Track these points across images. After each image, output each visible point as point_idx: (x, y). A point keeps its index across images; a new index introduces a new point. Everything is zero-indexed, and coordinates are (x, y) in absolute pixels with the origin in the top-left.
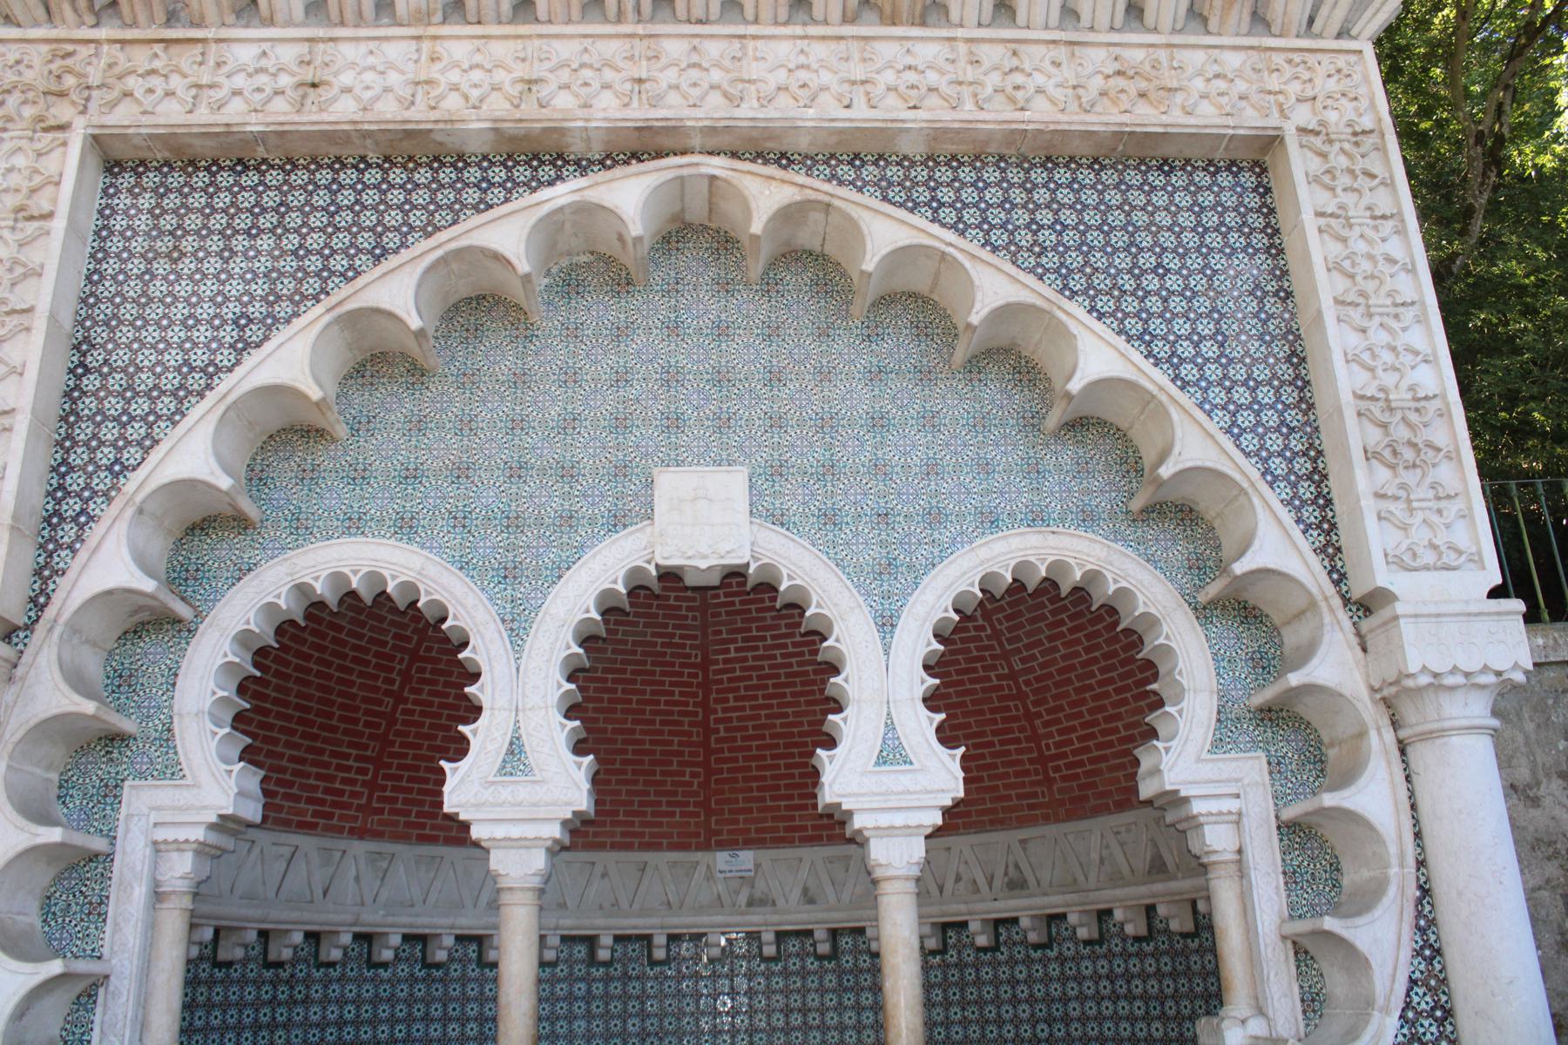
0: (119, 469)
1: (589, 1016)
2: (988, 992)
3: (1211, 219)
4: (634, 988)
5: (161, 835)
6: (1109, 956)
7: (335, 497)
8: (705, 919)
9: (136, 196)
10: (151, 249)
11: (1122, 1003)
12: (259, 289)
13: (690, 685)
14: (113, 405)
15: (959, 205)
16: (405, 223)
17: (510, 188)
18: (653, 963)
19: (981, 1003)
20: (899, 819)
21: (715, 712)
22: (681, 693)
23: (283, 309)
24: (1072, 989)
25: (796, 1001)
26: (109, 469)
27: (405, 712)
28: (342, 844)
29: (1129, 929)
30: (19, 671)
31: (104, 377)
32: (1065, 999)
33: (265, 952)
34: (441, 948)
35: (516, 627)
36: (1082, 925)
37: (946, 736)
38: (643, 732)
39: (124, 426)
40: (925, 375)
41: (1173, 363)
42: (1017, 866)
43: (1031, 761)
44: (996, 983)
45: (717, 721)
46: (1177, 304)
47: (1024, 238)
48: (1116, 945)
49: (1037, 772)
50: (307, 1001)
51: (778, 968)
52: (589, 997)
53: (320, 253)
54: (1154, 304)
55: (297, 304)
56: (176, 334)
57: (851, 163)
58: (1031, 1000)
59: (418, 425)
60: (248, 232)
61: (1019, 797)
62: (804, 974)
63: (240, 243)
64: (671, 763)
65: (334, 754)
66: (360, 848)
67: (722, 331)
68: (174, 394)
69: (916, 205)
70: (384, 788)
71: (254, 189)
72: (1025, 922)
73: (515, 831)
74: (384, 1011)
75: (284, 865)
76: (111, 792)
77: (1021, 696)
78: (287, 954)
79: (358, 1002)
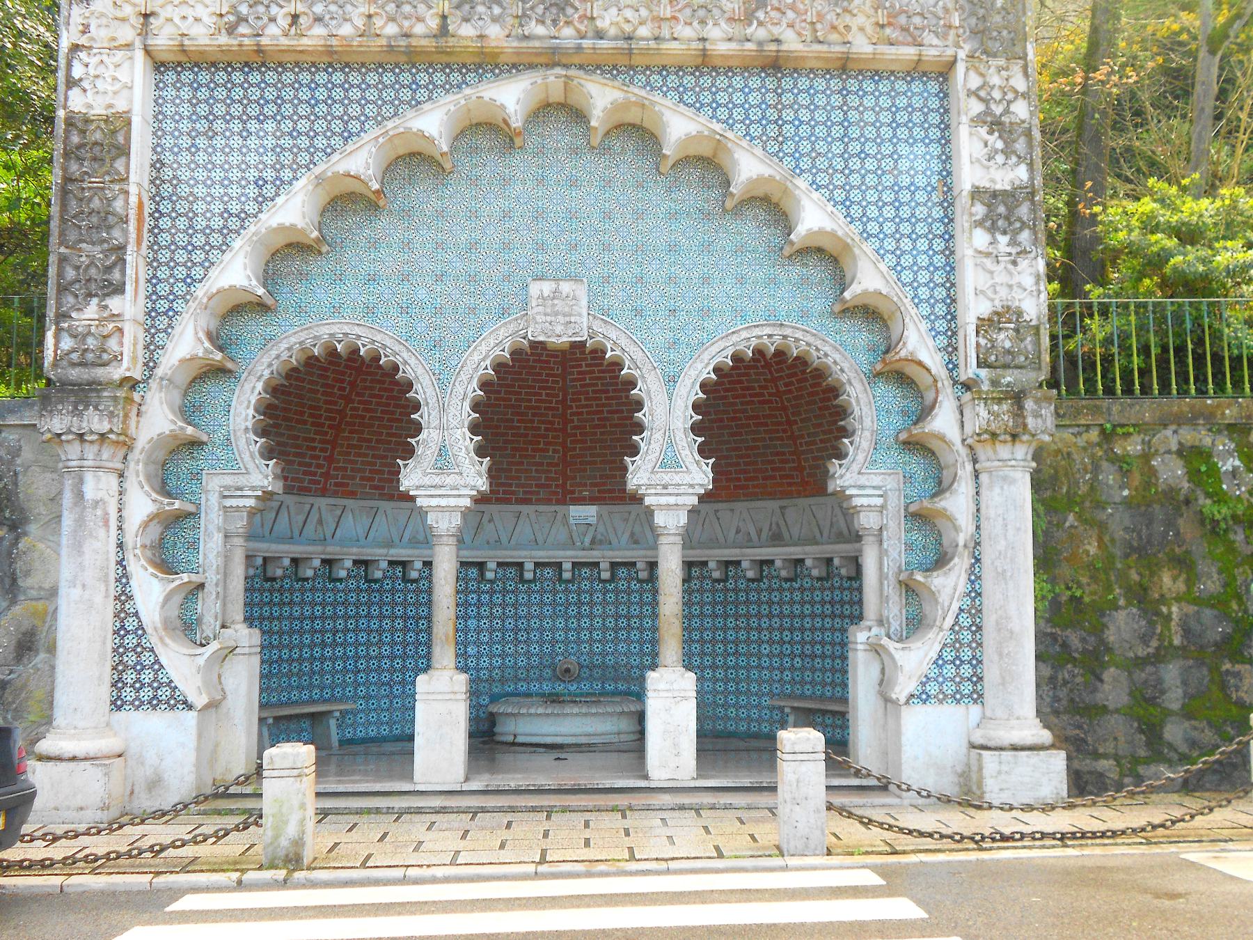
0: (190, 281)
1: (479, 617)
2: (753, 609)
3: (902, 117)
4: (510, 598)
5: (228, 503)
6: (832, 589)
7: (321, 294)
8: (561, 553)
9: (178, 90)
10: (193, 129)
11: (838, 620)
12: (269, 159)
13: (553, 389)
14: (182, 239)
15: (731, 106)
16: (363, 114)
17: (432, 87)
18: (522, 580)
19: (748, 616)
20: (672, 500)
21: (571, 407)
22: (547, 395)
23: (287, 174)
25: (623, 610)
27: (353, 409)
28: (311, 500)
29: (843, 572)
30: (143, 408)
31: (174, 219)
32: (802, 616)
33: (265, 571)
34: (378, 569)
35: (442, 385)
36: (815, 567)
37: (703, 451)
38: (519, 421)
39: (190, 253)
40: (707, 216)
41: (864, 219)
42: (778, 524)
43: (791, 453)
44: (759, 603)
45: (572, 414)
46: (871, 180)
47: (772, 130)
48: (836, 582)
49: (793, 461)
50: (291, 603)
51: (611, 587)
52: (479, 604)
54: (855, 179)
55: (295, 171)
56: (217, 191)
57: (660, 73)
58: (781, 616)
59: (374, 244)
60: (257, 118)
61: (782, 477)
62: (629, 592)
64: (539, 443)
65: (305, 439)
66: (322, 502)
67: (573, 183)
68: (220, 231)
69: (702, 105)
70: (339, 461)
71: (258, 85)
72: (778, 563)
73: (443, 502)
74: (341, 610)
75: (273, 515)
76: (196, 476)
77: (784, 409)
78: (279, 572)
79: (323, 605)
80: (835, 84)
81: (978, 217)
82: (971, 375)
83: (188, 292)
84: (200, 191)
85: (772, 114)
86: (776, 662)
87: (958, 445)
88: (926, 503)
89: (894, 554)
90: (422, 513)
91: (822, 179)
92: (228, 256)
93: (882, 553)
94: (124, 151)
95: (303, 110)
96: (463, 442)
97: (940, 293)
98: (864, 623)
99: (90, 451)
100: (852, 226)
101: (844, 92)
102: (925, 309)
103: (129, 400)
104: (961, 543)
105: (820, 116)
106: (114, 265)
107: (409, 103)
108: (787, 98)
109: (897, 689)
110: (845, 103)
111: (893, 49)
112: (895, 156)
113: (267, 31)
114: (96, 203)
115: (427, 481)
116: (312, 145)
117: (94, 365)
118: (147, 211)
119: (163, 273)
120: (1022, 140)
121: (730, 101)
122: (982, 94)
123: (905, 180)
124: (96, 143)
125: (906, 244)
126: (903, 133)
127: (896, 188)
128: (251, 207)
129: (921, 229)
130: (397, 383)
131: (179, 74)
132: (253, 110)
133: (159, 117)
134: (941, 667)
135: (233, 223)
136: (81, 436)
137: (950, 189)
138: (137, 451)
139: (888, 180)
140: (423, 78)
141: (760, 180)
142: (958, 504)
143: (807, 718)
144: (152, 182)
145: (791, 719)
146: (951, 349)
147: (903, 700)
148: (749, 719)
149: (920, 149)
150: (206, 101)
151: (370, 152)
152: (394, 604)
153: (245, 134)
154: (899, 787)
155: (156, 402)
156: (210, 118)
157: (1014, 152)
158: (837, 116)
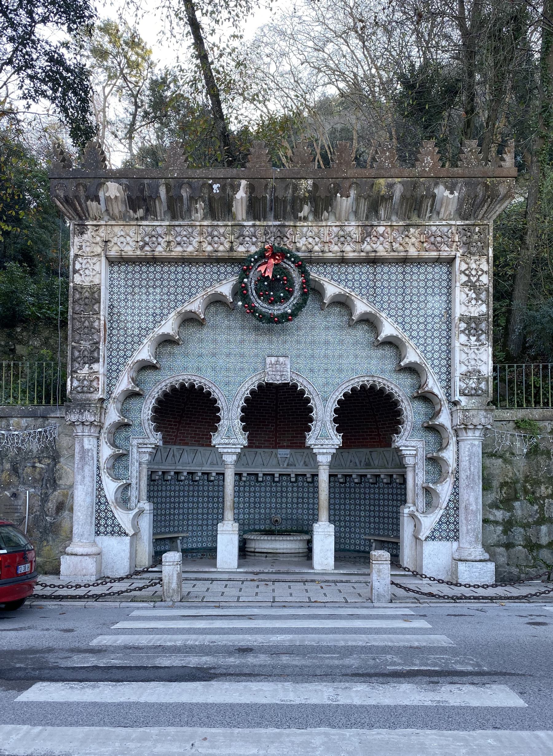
0: (126, 357)
10: (126, 291)
17: (226, 273)
23: (165, 311)
24: (381, 497)
26: (123, 357)
30: (107, 411)
31: (119, 330)
46: (414, 312)
47: (371, 291)
53: (174, 294)
54: (407, 312)
55: (169, 310)
56: (136, 318)
60: (153, 287)
63: (151, 290)
68: (138, 336)
71: (153, 272)
73: (229, 450)
80: (400, 269)
81: (462, 329)
82: (457, 399)
83: (125, 362)
84: (129, 318)
85: (371, 284)
86: (367, 520)
87: (450, 430)
88: (435, 454)
89: (420, 475)
90: (221, 454)
91: (393, 312)
92: (141, 346)
93: (415, 475)
94: (98, 301)
95: (172, 283)
96: (238, 424)
97: (444, 362)
98: (407, 505)
99: (86, 429)
100: (405, 334)
101: (404, 273)
102: (437, 370)
103: (101, 408)
104: (450, 472)
105: (393, 284)
106: (94, 350)
107: (216, 280)
108: (379, 277)
109: (421, 534)
110: (404, 278)
111: (427, 254)
112: (426, 302)
113: (157, 249)
114: (87, 324)
115: (222, 441)
116: (176, 299)
117: (87, 392)
118: (107, 327)
119: (114, 353)
120: (484, 293)
121: (353, 278)
122: (467, 272)
123: (430, 312)
124: (86, 298)
125: (429, 341)
126: (430, 291)
127: (426, 316)
128: (151, 325)
129: (436, 334)
130: (211, 400)
131: (119, 267)
132: (151, 283)
133: (111, 286)
134: (440, 525)
135: (143, 332)
136: (83, 423)
137: (450, 316)
138: (105, 429)
139: (422, 312)
140: (222, 269)
141: (366, 313)
142: (449, 455)
143: (382, 545)
144: (109, 314)
145: (374, 545)
146: (448, 388)
147: (423, 538)
148: (355, 544)
149: (437, 298)
150: (131, 279)
151: (200, 302)
152: (204, 491)
153: (148, 294)
154: (421, 576)
155: (112, 408)
156: (133, 286)
157: (480, 299)
158: (401, 284)
